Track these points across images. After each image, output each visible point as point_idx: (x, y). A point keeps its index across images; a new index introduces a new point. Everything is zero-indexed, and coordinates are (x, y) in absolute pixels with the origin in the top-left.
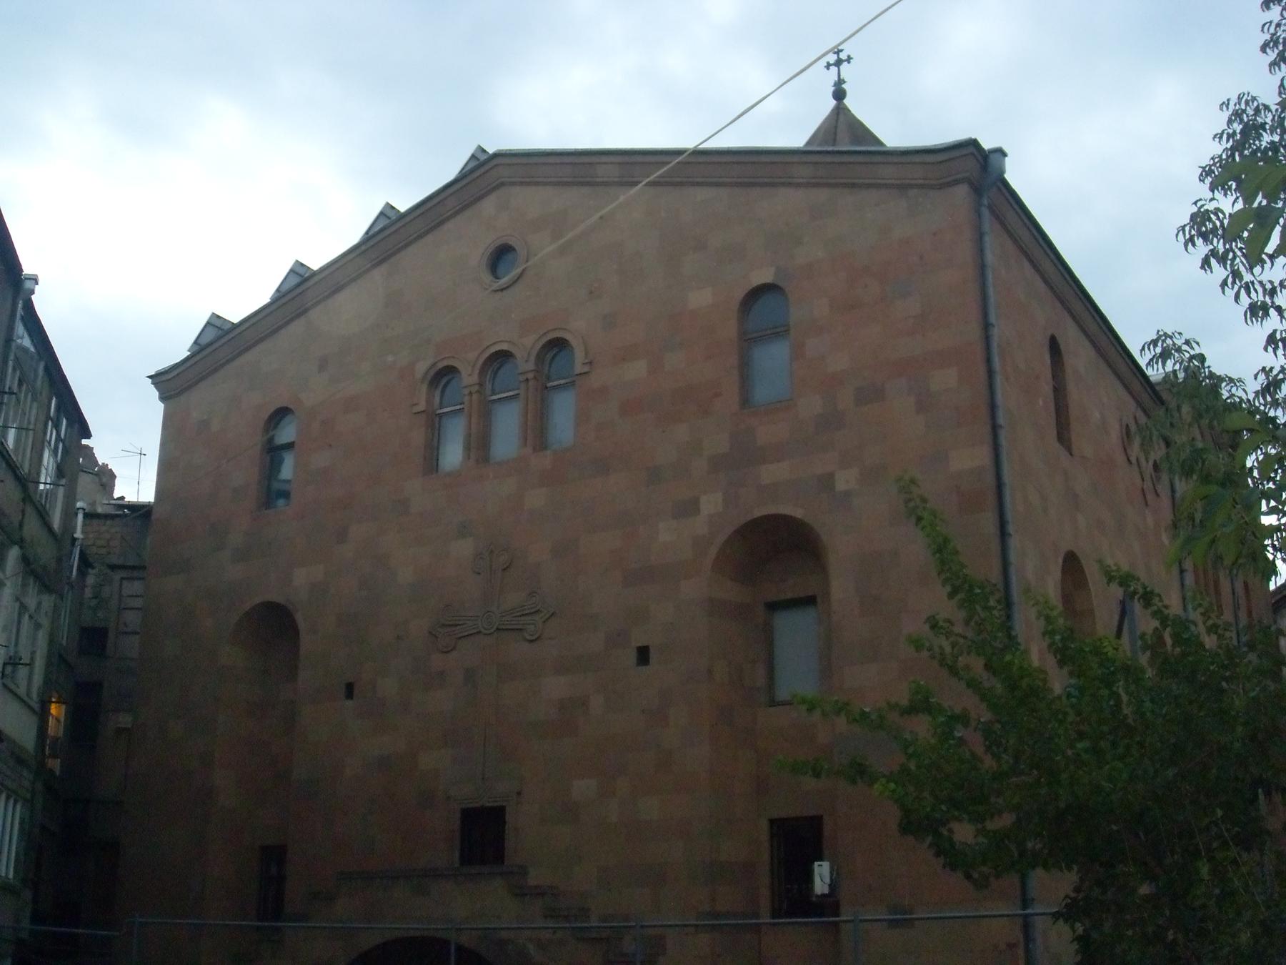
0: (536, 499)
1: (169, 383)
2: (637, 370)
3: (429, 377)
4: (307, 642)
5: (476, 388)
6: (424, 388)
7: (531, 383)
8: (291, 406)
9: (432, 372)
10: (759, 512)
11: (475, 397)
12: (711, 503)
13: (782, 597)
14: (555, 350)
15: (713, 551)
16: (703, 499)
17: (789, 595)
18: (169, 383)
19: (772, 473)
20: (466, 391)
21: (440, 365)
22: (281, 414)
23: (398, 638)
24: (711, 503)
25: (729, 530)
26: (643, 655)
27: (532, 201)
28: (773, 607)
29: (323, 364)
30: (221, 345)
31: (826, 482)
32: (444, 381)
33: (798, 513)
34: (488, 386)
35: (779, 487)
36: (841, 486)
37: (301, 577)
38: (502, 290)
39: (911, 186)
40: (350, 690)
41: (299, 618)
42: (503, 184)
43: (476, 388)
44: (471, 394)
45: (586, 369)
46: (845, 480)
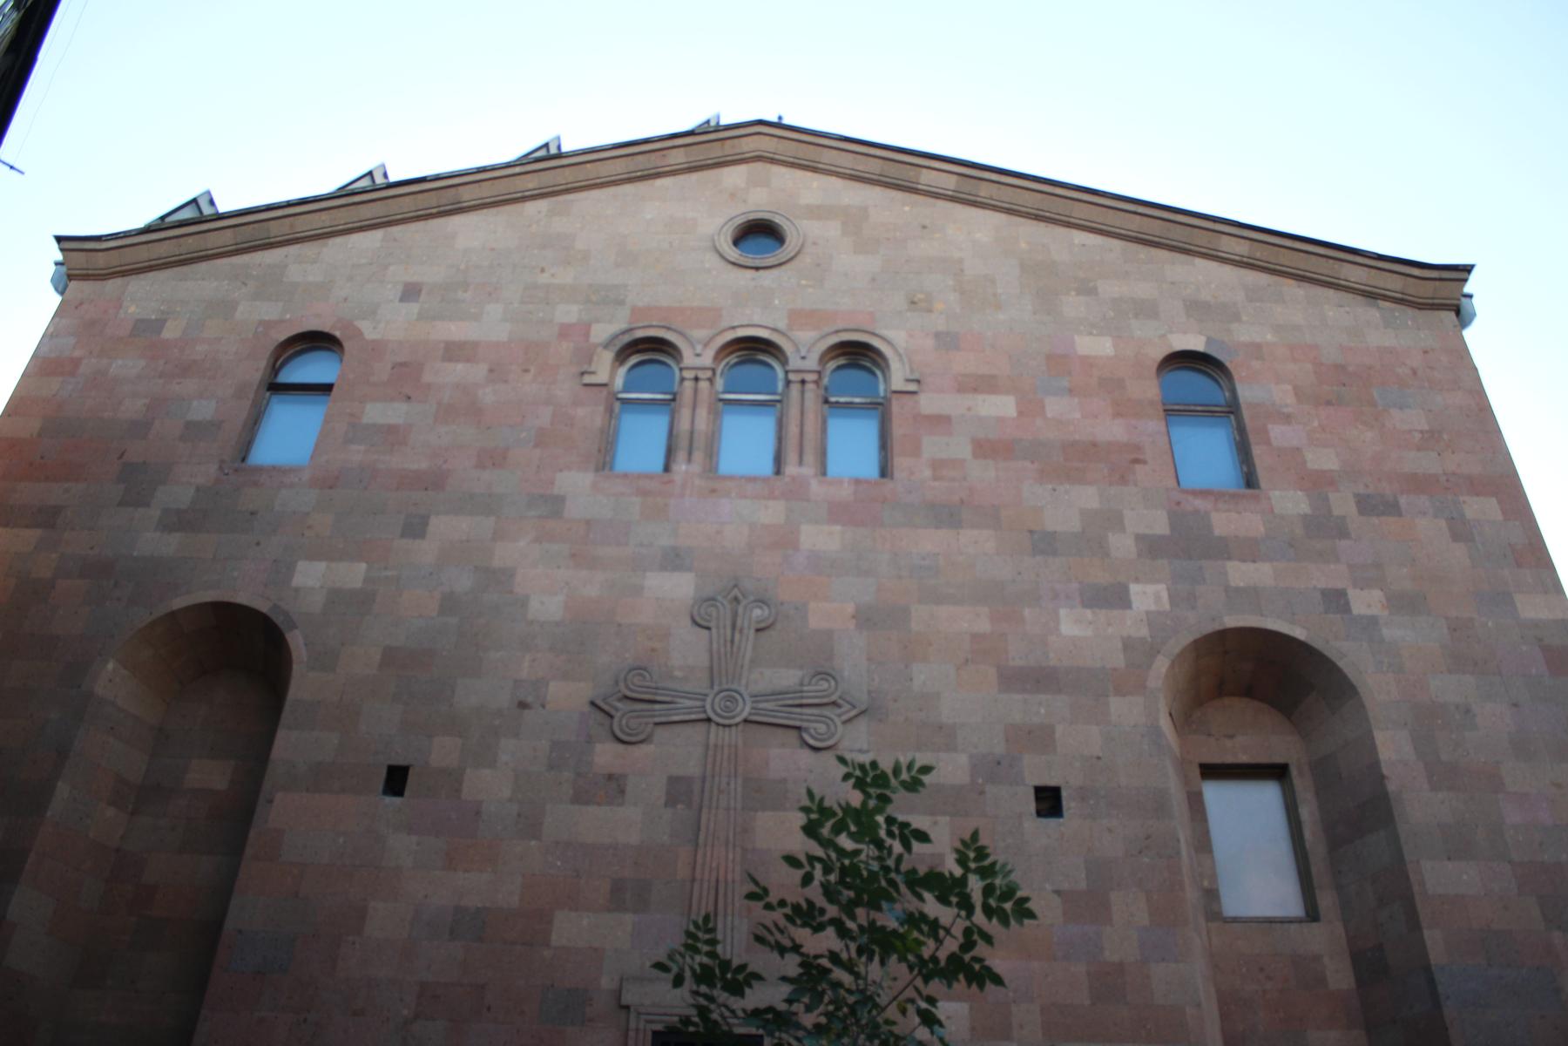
0: (821, 538)
1: (86, 261)
2: (1003, 406)
3: (619, 344)
4: (303, 684)
5: (709, 374)
6: (608, 356)
7: (810, 387)
8: (337, 334)
9: (627, 339)
10: (1232, 621)
11: (704, 385)
12: (1148, 596)
13: (1229, 759)
14: (842, 361)
15: (1162, 665)
16: (1134, 588)
17: (1244, 758)
18: (86, 261)
19: (1240, 573)
20: (688, 374)
21: (640, 334)
22: (318, 341)
23: (523, 705)
24: (1148, 596)
25: (1186, 639)
26: (1049, 801)
27: (811, 189)
28: (1212, 771)
29: (411, 292)
30: (192, 236)
31: (1336, 600)
32: (634, 360)
33: (1299, 633)
34: (720, 383)
35: (1264, 593)
36: (1358, 608)
37: (311, 576)
38: (757, 269)
39: (1385, 298)
40: (396, 780)
41: (296, 641)
42: (759, 158)
43: (709, 374)
44: (696, 379)
45: (912, 387)
46: (1365, 602)
